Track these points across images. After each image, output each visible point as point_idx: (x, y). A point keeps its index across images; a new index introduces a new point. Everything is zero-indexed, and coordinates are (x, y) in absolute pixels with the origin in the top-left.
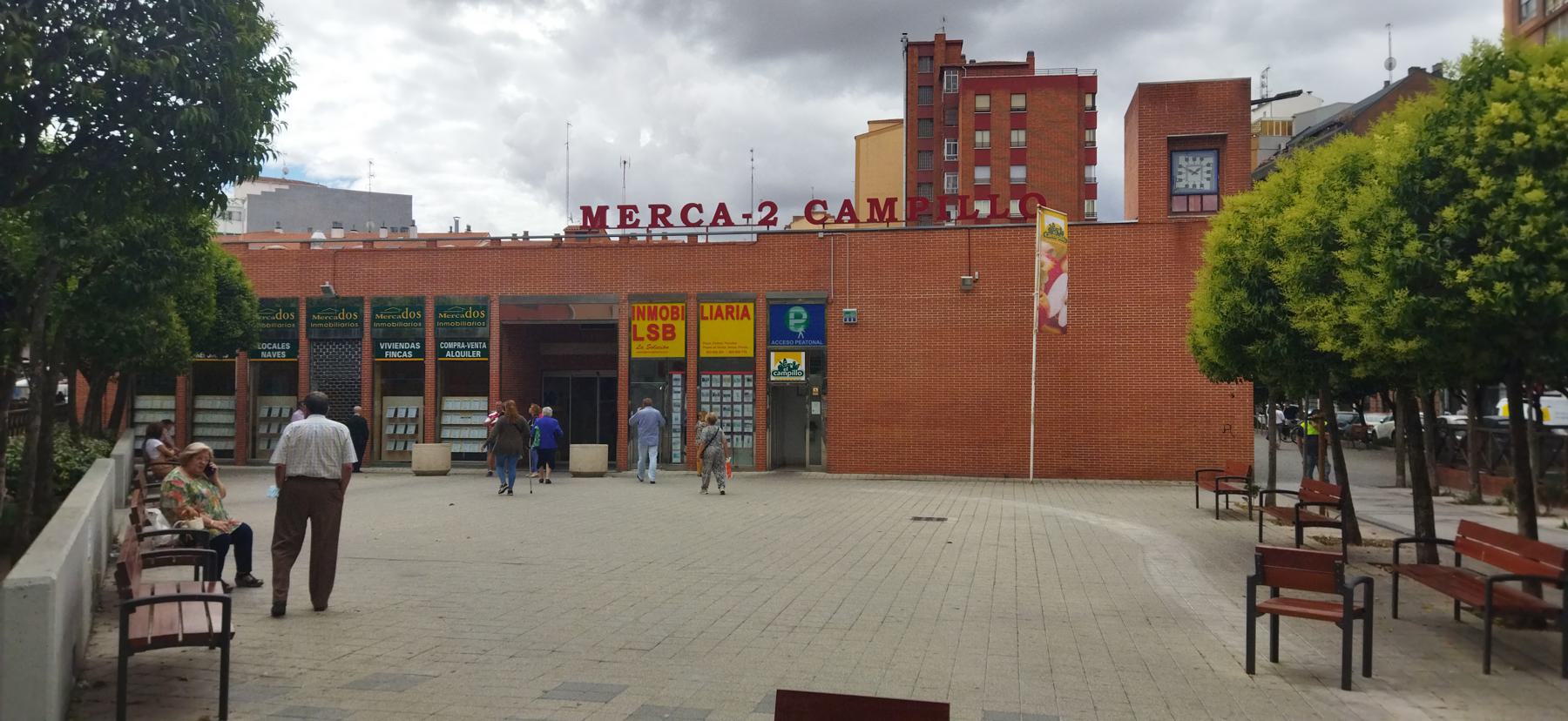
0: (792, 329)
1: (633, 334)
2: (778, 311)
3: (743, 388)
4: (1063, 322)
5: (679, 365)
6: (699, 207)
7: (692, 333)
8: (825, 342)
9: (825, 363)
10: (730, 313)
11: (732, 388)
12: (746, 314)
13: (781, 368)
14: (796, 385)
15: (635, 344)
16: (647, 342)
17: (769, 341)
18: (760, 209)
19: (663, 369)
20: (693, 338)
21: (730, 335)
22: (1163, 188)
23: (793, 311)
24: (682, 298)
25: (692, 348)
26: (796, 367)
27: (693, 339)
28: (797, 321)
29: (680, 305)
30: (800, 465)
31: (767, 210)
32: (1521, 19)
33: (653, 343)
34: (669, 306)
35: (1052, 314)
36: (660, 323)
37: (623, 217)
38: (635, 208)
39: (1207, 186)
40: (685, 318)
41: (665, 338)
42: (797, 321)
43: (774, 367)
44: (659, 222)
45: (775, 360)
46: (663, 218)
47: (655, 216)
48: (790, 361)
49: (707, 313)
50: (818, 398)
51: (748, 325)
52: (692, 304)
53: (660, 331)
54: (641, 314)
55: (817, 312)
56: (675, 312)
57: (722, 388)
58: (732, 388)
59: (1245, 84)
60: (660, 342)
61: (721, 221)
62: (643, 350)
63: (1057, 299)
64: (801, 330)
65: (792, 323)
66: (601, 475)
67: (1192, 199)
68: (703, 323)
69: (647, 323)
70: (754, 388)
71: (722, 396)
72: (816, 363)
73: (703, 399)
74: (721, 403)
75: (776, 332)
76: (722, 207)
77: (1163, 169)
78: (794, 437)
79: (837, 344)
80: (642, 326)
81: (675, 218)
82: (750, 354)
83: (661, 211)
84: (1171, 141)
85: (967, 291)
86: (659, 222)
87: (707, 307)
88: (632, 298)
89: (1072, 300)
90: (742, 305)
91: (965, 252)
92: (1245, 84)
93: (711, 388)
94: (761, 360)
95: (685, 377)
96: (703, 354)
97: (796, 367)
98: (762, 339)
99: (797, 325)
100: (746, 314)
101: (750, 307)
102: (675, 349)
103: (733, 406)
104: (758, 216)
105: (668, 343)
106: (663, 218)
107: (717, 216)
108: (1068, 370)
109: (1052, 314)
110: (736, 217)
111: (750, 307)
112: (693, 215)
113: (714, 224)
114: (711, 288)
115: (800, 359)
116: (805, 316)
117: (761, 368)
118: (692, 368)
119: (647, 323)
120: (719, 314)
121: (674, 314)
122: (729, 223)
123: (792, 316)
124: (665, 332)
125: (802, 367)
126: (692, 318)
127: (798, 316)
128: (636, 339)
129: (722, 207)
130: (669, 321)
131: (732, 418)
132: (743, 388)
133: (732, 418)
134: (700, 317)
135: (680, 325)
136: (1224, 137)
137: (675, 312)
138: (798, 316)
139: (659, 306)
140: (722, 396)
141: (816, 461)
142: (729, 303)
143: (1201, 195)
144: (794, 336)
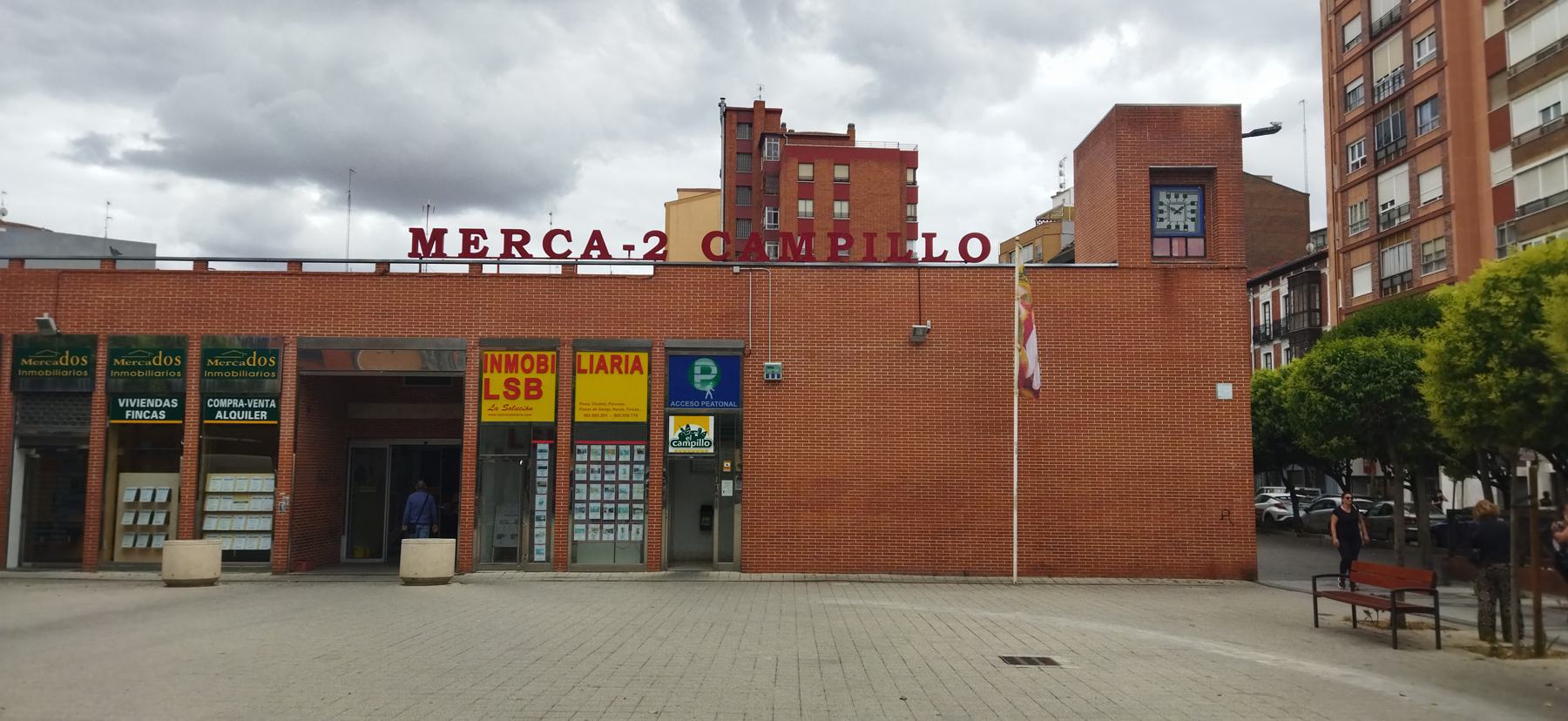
0: (698, 386)
1: (483, 390)
2: (678, 366)
3: (632, 463)
4: (1036, 384)
5: (547, 432)
6: (567, 235)
7: (566, 391)
8: (739, 403)
9: (741, 433)
10: (616, 365)
11: (617, 463)
12: (637, 366)
13: (682, 437)
14: (705, 457)
15: (486, 404)
16: (503, 401)
17: (667, 404)
18: (646, 240)
19: (517, 440)
20: (565, 396)
21: (614, 393)
22: (1146, 230)
23: (699, 364)
24: (552, 345)
25: (564, 410)
26: (702, 436)
27: (566, 398)
28: (704, 377)
29: (549, 354)
30: (706, 561)
31: (655, 241)
32: (1347, 106)
33: (511, 403)
34: (535, 354)
35: (1028, 375)
36: (521, 376)
37: (467, 243)
38: (482, 232)
39: (1192, 228)
40: (556, 369)
41: (528, 397)
42: (704, 377)
43: (673, 435)
44: (514, 251)
45: (675, 427)
46: (519, 246)
47: (508, 243)
48: (694, 428)
49: (585, 364)
50: (728, 476)
51: (640, 380)
52: (566, 352)
53: (522, 387)
54: (496, 364)
55: (731, 367)
56: (542, 362)
57: (603, 463)
58: (617, 463)
59: (1234, 112)
60: (521, 401)
61: (595, 253)
62: (496, 411)
63: (1029, 355)
64: (709, 388)
65: (698, 379)
66: (444, 581)
67: (1175, 242)
68: (578, 376)
69: (505, 376)
70: (647, 463)
71: (603, 472)
72: (729, 432)
73: (578, 477)
74: (602, 482)
75: (677, 389)
76: (597, 235)
77: (1145, 206)
78: (698, 523)
79: (756, 408)
80: (497, 381)
81: (535, 248)
82: (643, 418)
83: (517, 238)
84: (1154, 173)
85: (918, 344)
86: (514, 251)
87: (585, 358)
88: (485, 343)
89: (1042, 355)
90: (632, 356)
91: (914, 295)
92: (1234, 112)
93: (589, 462)
94: (656, 427)
95: (553, 448)
96: (579, 417)
97: (702, 436)
98: (659, 397)
99: (704, 382)
100: (637, 366)
101: (644, 357)
102: (542, 411)
103: (611, 487)
104: (642, 250)
105: (531, 403)
106: (519, 246)
107: (590, 247)
108: (1038, 442)
109: (1028, 375)
110: (615, 250)
111: (644, 357)
112: (559, 245)
113: (586, 255)
114: (591, 333)
115: (708, 425)
116: (715, 370)
117: (656, 437)
118: (564, 435)
119: (505, 376)
120: (602, 366)
121: (542, 367)
122: (605, 255)
123: (697, 370)
124: (528, 389)
125: (710, 436)
126: (566, 370)
127: (706, 371)
128: (489, 397)
129: (597, 235)
130: (534, 375)
131: (617, 501)
132: (632, 463)
133: (617, 501)
134: (576, 369)
135: (548, 381)
136: (1210, 173)
137: (542, 362)
138: (706, 371)
139: (521, 354)
140: (603, 472)
141: (727, 557)
142: (613, 351)
143: (1186, 237)
144: (700, 395)
